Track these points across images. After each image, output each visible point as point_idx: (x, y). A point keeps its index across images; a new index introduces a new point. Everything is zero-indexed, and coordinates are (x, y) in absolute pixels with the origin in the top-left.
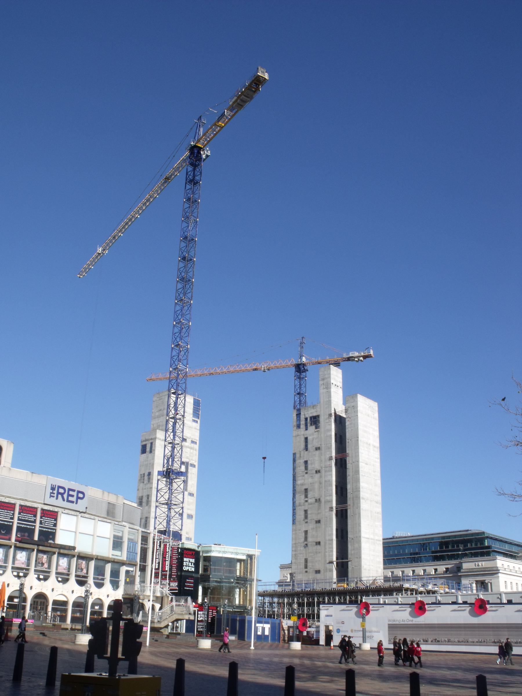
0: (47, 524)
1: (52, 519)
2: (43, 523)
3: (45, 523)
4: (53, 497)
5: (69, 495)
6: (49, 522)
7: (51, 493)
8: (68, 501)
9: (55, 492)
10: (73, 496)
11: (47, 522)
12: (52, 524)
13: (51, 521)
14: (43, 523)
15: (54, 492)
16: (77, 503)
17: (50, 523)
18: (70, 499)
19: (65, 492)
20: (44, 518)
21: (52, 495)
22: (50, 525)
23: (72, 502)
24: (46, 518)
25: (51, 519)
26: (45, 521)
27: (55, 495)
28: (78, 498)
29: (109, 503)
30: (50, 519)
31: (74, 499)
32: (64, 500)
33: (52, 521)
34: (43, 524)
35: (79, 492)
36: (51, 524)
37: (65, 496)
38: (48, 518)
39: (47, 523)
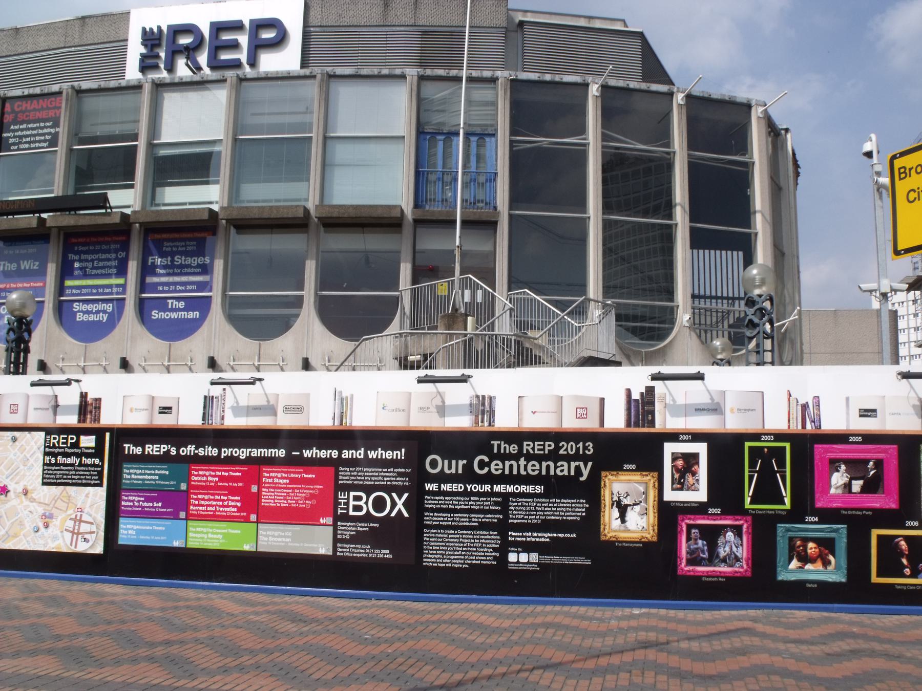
0: (27, 146)
1: (45, 121)
2: (14, 144)
3: (20, 143)
6: (34, 135)
11: (26, 136)
12: (45, 141)
13: (40, 131)
14: (14, 144)
17: (38, 138)
20: (17, 127)
22: (37, 145)
24: (24, 126)
25: (42, 124)
26: (20, 137)
29: (425, 33)
30: (37, 125)
33: (45, 131)
34: (13, 148)
36: (40, 142)
38: (29, 122)
39: (28, 139)
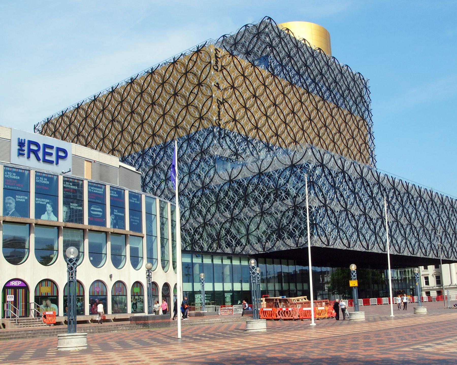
4: (23, 155)
5: (45, 153)
7: (19, 150)
8: (45, 161)
9: (26, 148)
10: (51, 154)
15: (23, 148)
16: (57, 163)
18: (47, 158)
19: (39, 150)
21: (21, 152)
23: (51, 162)
27: (26, 152)
28: (58, 157)
31: (53, 158)
32: (38, 159)
35: (59, 149)
37: (40, 154)
